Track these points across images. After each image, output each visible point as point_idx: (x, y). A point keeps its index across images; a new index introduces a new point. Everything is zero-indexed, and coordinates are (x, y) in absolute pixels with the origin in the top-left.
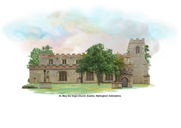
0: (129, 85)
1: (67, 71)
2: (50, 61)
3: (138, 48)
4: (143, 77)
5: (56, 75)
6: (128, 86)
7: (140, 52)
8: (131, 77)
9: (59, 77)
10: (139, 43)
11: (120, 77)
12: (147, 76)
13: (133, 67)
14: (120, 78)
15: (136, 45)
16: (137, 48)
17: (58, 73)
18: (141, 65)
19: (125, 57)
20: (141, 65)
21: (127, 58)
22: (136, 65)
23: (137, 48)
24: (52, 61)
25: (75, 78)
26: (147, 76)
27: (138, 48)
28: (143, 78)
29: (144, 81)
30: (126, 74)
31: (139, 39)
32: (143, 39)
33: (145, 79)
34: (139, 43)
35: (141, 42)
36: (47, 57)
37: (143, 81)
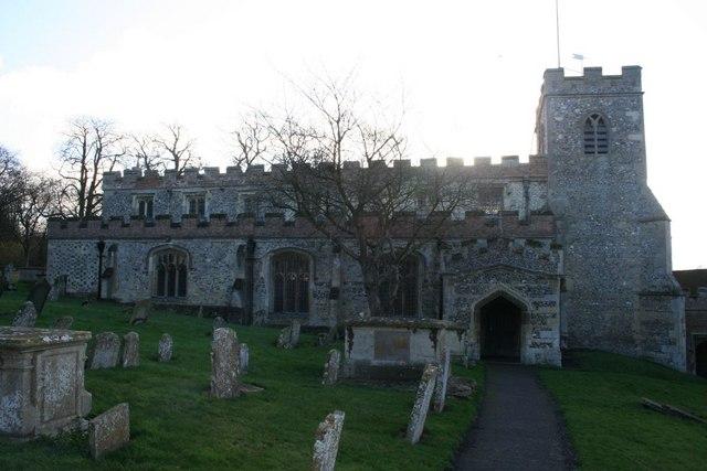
0: (534, 345)
1: (190, 245)
2: (142, 204)
3: (595, 123)
5: (142, 268)
8: (549, 291)
9: (156, 276)
10: (601, 95)
11: (467, 290)
12: (667, 294)
13: (568, 237)
15: (585, 106)
16: (588, 121)
17: (151, 259)
18: (622, 225)
22: (585, 227)
24: (150, 204)
25: (223, 287)
26: (667, 294)
27: (595, 123)
28: (637, 306)
29: (645, 323)
30: (509, 268)
31: (605, 73)
32: (632, 74)
34: (601, 95)
36: (131, 187)
37: (635, 327)
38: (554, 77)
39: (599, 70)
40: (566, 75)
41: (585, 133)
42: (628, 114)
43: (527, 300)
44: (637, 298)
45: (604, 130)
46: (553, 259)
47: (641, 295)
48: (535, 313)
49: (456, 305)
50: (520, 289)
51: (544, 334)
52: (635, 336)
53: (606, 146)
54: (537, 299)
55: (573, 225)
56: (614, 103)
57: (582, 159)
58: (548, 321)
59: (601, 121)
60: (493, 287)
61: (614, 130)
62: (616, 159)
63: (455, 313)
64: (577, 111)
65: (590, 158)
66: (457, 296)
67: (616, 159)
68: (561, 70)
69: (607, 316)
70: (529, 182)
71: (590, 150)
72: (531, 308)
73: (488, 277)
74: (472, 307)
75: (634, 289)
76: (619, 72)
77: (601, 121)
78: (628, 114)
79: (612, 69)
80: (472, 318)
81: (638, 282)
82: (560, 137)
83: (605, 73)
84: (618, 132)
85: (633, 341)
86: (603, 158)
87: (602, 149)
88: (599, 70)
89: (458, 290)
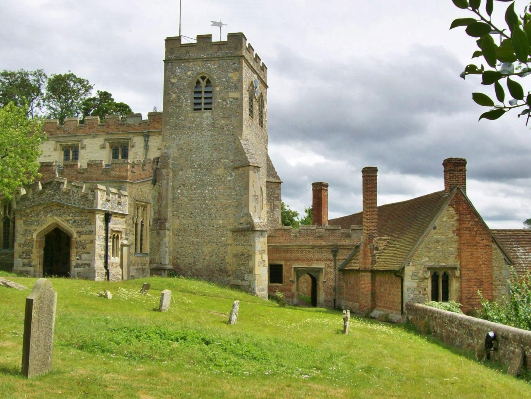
0: (78, 266)
3: (203, 83)
4: (229, 238)
6: (74, 270)
7: (213, 106)
10: (209, 59)
11: (32, 223)
12: (248, 230)
14: (32, 228)
16: (198, 82)
18: (220, 171)
19: (137, 133)
20: (220, 171)
21: (147, 137)
23: (198, 82)
28: (230, 241)
29: (235, 256)
30: (60, 206)
31: (215, 39)
33: (240, 249)
35: (220, 54)
37: (229, 259)
38: (173, 43)
39: (209, 37)
40: (182, 43)
41: (195, 92)
42: (230, 75)
43: (73, 231)
44: (230, 234)
45: (209, 89)
46: (90, 197)
47: (234, 231)
48: (78, 239)
49: (24, 235)
50: (68, 221)
51: (84, 256)
52: (229, 268)
53: (211, 103)
54: (80, 229)
55: (181, 173)
56: (219, 66)
57: (190, 115)
58: (88, 246)
59: (208, 82)
60: (50, 220)
61: (218, 89)
62: (218, 114)
63: (23, 242)
64: (189, 73)
65: (197, 114)
66: (25, 227)
67: (218, 114)
68: (179, 39)
69: (206, 249)
70: (148, 136)
71: (198, 107)
72: (75, 235)
73: (46, 214)
74: (35, 236)
75: (228, 227)
76: (225, 39)
77: (208, 82)
78: (230, 75)
79: (219, 36)
80: (34, 246)
81: (232, 220)
82: (174, 96)
83: (215, 39)
84: (221, 91)
85: (226, 272)
86: (208, 114)
87: (208, 106)
88: (209, 37)
89: (25, 222)
